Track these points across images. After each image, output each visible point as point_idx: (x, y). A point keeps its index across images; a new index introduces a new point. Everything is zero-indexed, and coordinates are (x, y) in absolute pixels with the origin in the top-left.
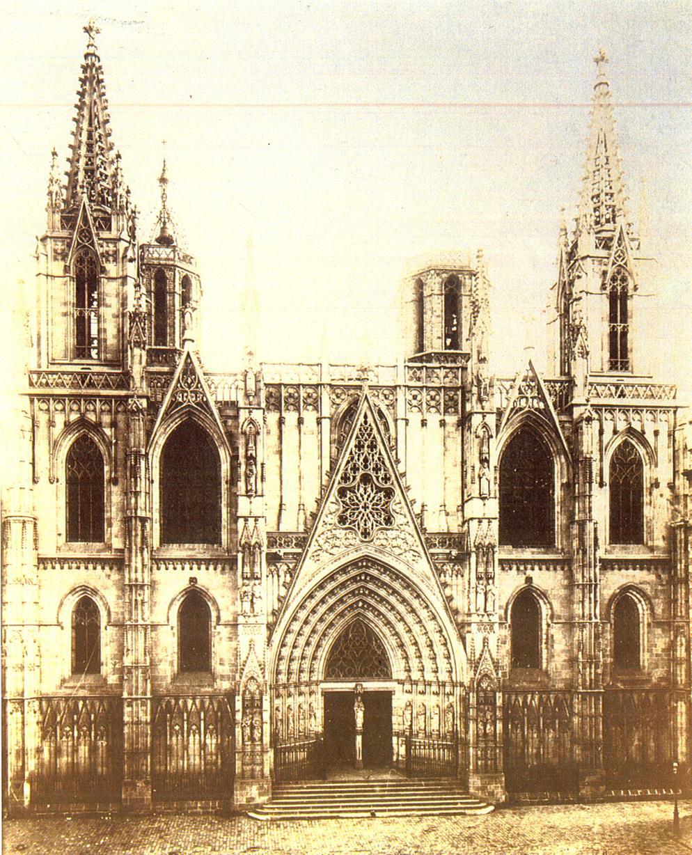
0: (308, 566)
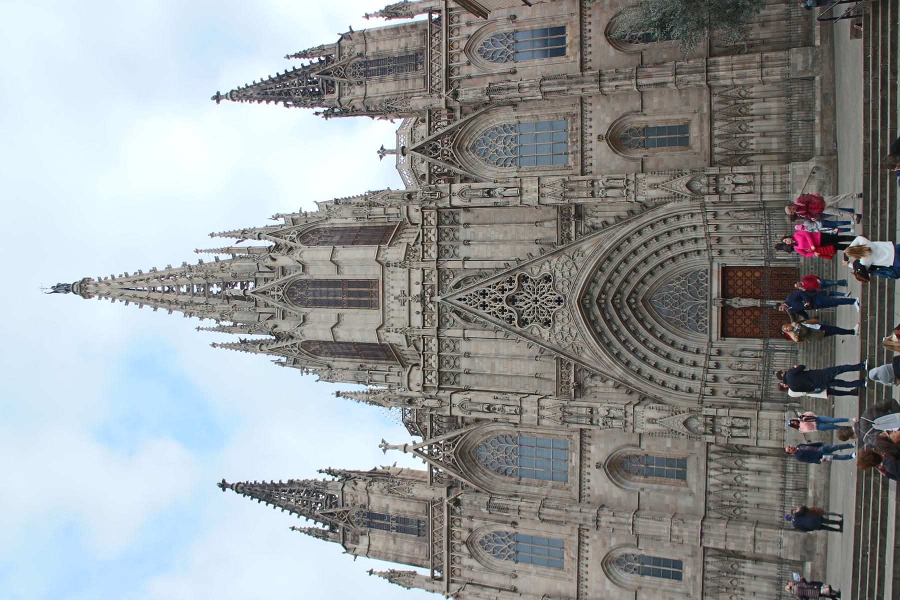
0: (586, 356)
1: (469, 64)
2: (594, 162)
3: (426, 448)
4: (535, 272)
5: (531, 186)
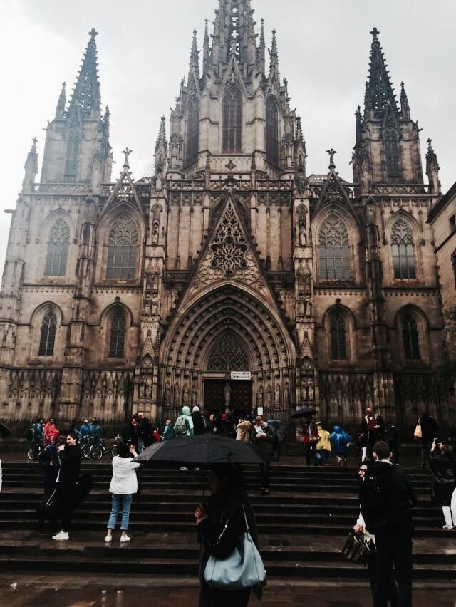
0: (192, 290)
1: (392, 212)
2: (321, 296)
3: (127, 182)
4: (249, 257)
5: (306, 253)
